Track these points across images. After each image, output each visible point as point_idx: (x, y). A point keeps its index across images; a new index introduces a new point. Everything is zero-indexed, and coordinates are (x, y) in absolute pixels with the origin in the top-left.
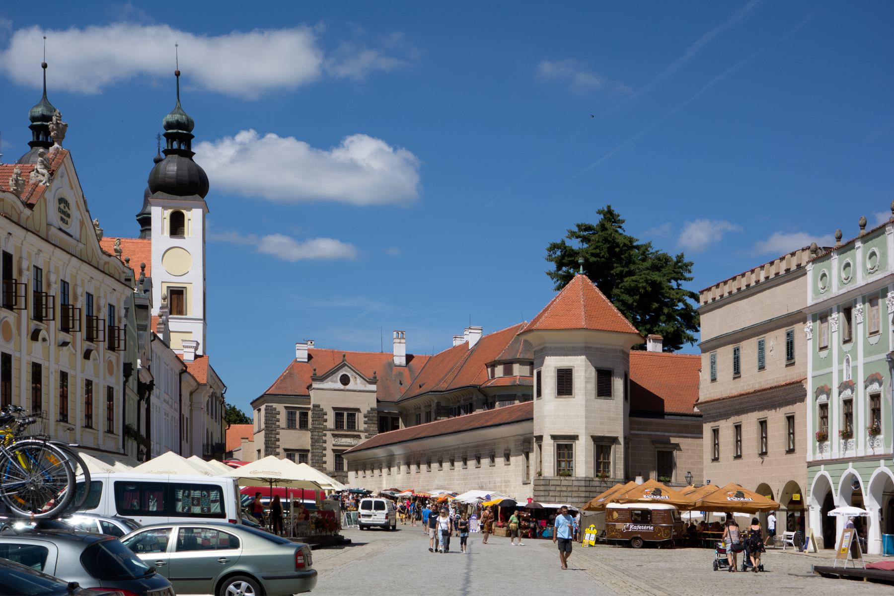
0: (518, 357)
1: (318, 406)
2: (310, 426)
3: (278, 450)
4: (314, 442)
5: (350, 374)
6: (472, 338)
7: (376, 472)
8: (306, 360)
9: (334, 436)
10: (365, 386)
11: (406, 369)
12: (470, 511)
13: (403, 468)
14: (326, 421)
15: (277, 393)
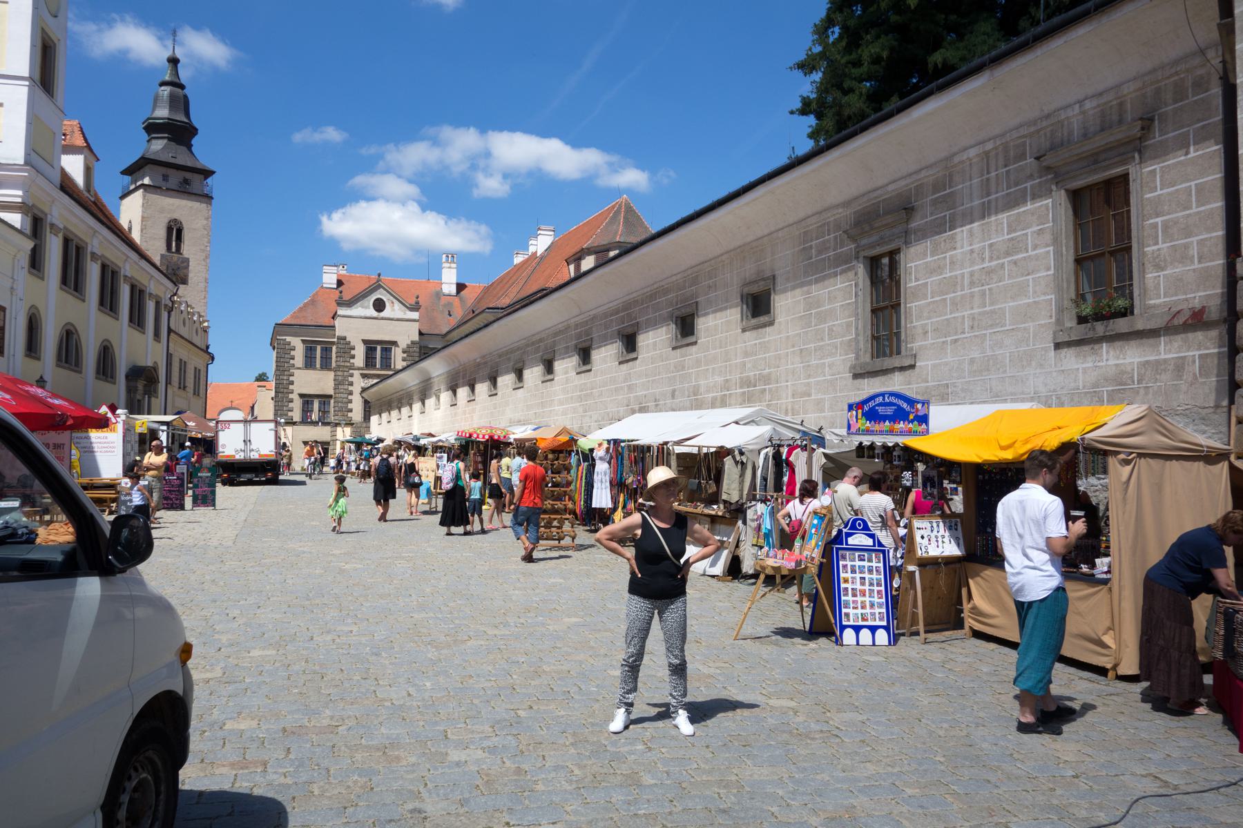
0: (618, 239)
1: (345, 338)
2: (334, 365)
3: (291, 396)
4: (338, 383)
5: (385, 297)
6: (541, 243)
7: (405, 410)
8: (335, 286)
9: (364, 376)
10: (405, 314)
11: (456, 299)
12: (736, 485)
13: (445, 396)
14: (353, 357)
15: (293, 323)
